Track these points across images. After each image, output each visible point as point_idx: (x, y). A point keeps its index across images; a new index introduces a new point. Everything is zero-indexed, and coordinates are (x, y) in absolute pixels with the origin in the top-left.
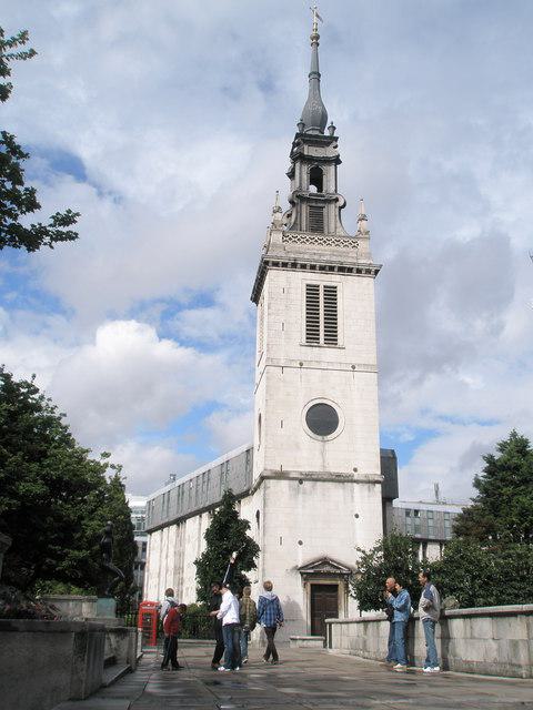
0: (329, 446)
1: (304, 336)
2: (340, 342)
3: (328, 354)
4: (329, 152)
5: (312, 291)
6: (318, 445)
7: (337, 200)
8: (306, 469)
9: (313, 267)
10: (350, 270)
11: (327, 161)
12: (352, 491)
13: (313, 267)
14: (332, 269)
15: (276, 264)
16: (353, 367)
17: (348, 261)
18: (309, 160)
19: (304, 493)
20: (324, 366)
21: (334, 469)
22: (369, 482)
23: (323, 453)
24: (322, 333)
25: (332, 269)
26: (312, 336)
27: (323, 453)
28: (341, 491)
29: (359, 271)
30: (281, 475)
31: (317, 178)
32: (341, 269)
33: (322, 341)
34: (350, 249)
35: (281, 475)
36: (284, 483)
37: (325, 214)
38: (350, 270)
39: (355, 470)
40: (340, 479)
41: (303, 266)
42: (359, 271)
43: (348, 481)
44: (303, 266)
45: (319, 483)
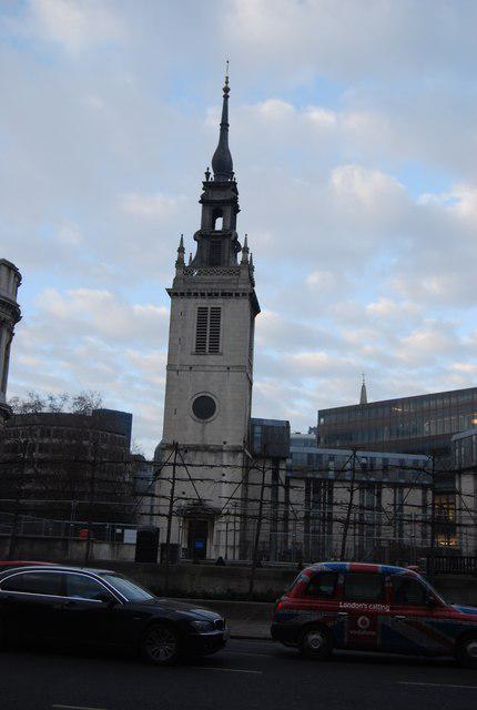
0: (208, 426)
3: (212, 359)
5: (202, 311)
6: (200, 425)
8: (191, 442)
10: (230, 295)
13: (203, 295)
14: (217, 295)
17: (228, 288)
20: (208, 368)
21: (212, 441)
23: (202, 431)
24: (207, 345)
25: (217, 295)
26: (200, 349)
27: (202, 431)
29: (237, 295)
32: (224, 294)
34: (234, 277)
38: (230, 295)
39: (225, 443)
40: (218, 451)
41: (196, 294)
42: (237, 295)
44: (196, 294)
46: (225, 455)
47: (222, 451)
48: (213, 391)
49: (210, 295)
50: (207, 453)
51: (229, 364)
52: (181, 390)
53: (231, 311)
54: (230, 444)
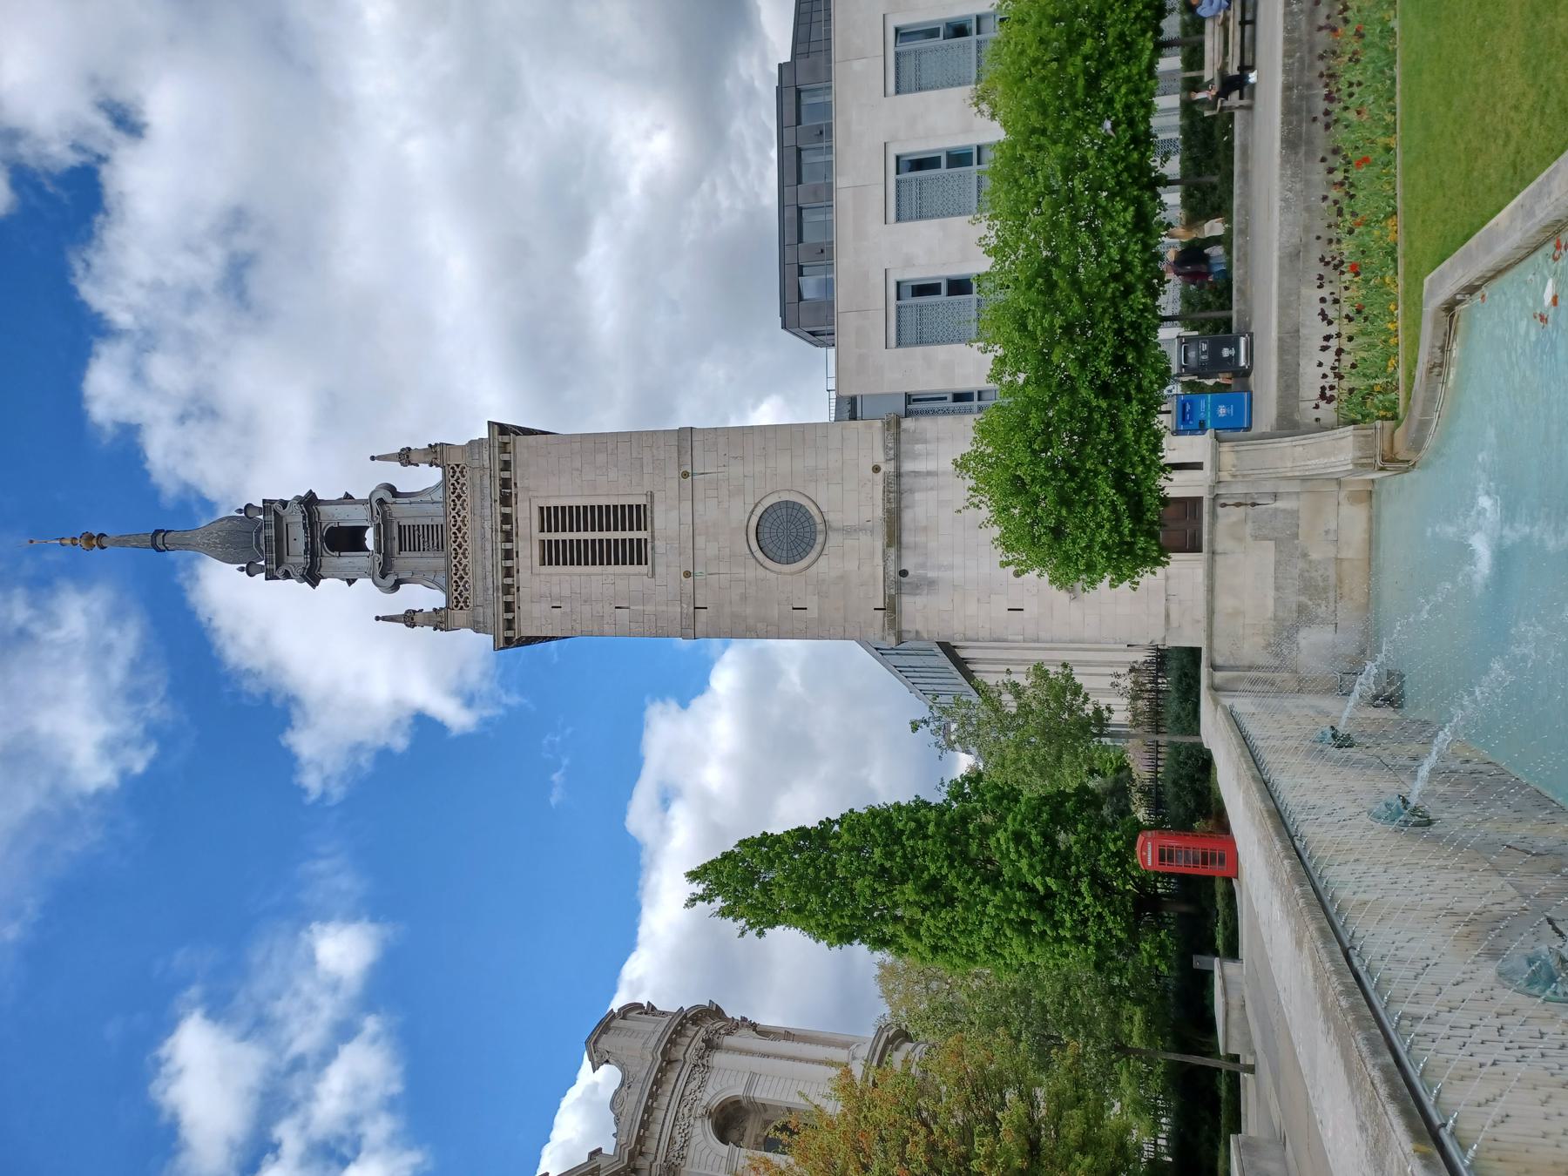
1: (635, 568)
2: (642, 501)
3: (666, 522)
4: (295, 518)
5: (552, 554)
6: (834, 539)
7: (381, 502)
9: (508, 555)
10: (505, 483)
11: (311, 522)
12: (916, 474)
13: (508, 555)
14: (506, 519)
15: (509, 624)
16: (685, 475)
18: (312, 552)
19: (923, 566)
21: (875, 511)
22: (898, 441)
23: (848, 531)
25: (506, 519)
26: (635, 553)
27: (848, 531)
28: (918, 496)
30: (891, 609)
31: (349, 539)
33: (641, 535)
35: (891, 609)
36: (909, 604)
37: (410, 522)
38: (505, 483)
39: (876, 469)
41: (508, 572)
42: (506, 466)
43: (899, 484)
45: (907, 538)
46: (908, 466)
47: (898, 475)
48: (740, 513)
49: (508, 537)
50: (907, 517)
51: (676, 474)
52: (744, 598)
53: (542, 488)
54: (879, 458)
